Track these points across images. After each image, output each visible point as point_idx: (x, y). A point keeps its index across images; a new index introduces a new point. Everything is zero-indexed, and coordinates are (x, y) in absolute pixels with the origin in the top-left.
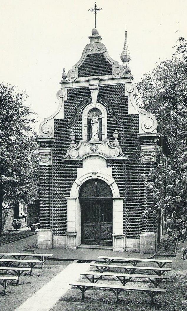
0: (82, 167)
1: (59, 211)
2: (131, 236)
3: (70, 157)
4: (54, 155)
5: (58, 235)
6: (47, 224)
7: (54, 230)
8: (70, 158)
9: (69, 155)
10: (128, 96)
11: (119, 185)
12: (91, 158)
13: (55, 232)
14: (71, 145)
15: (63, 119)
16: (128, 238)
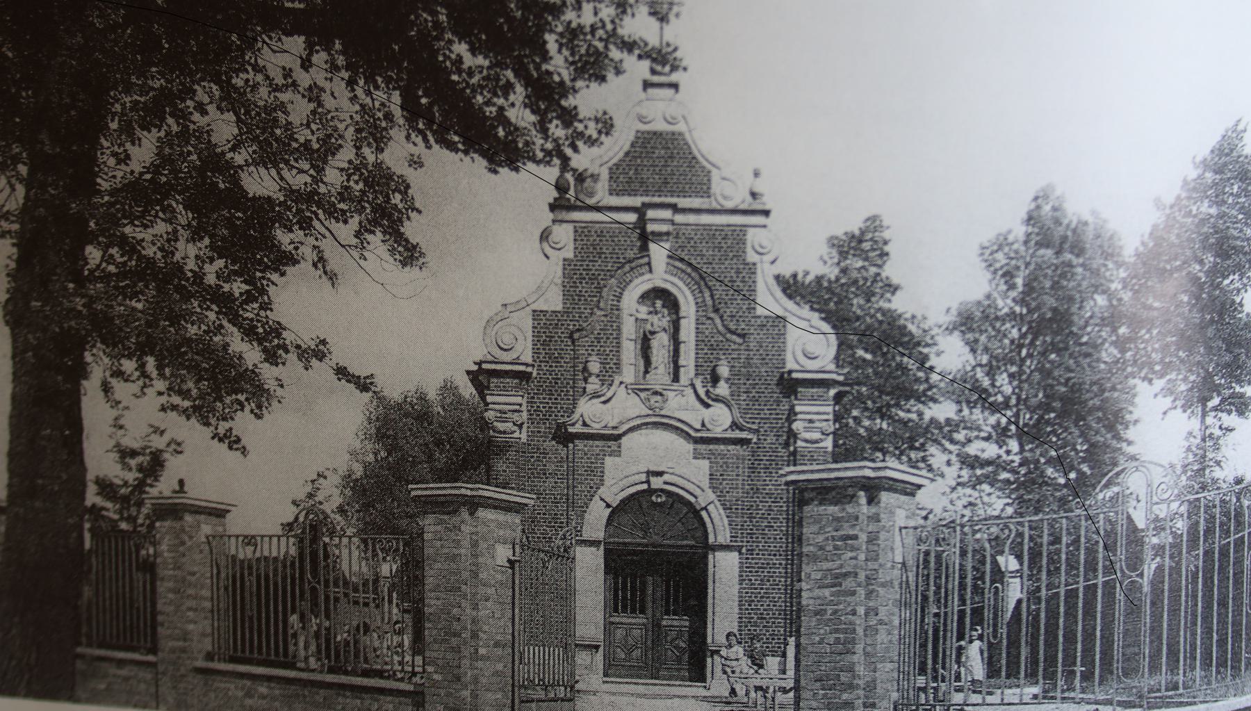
3: (584, 421)
8: (585, 424)
10: (754, 264)
12: (665, 429)
14: (590, 388)
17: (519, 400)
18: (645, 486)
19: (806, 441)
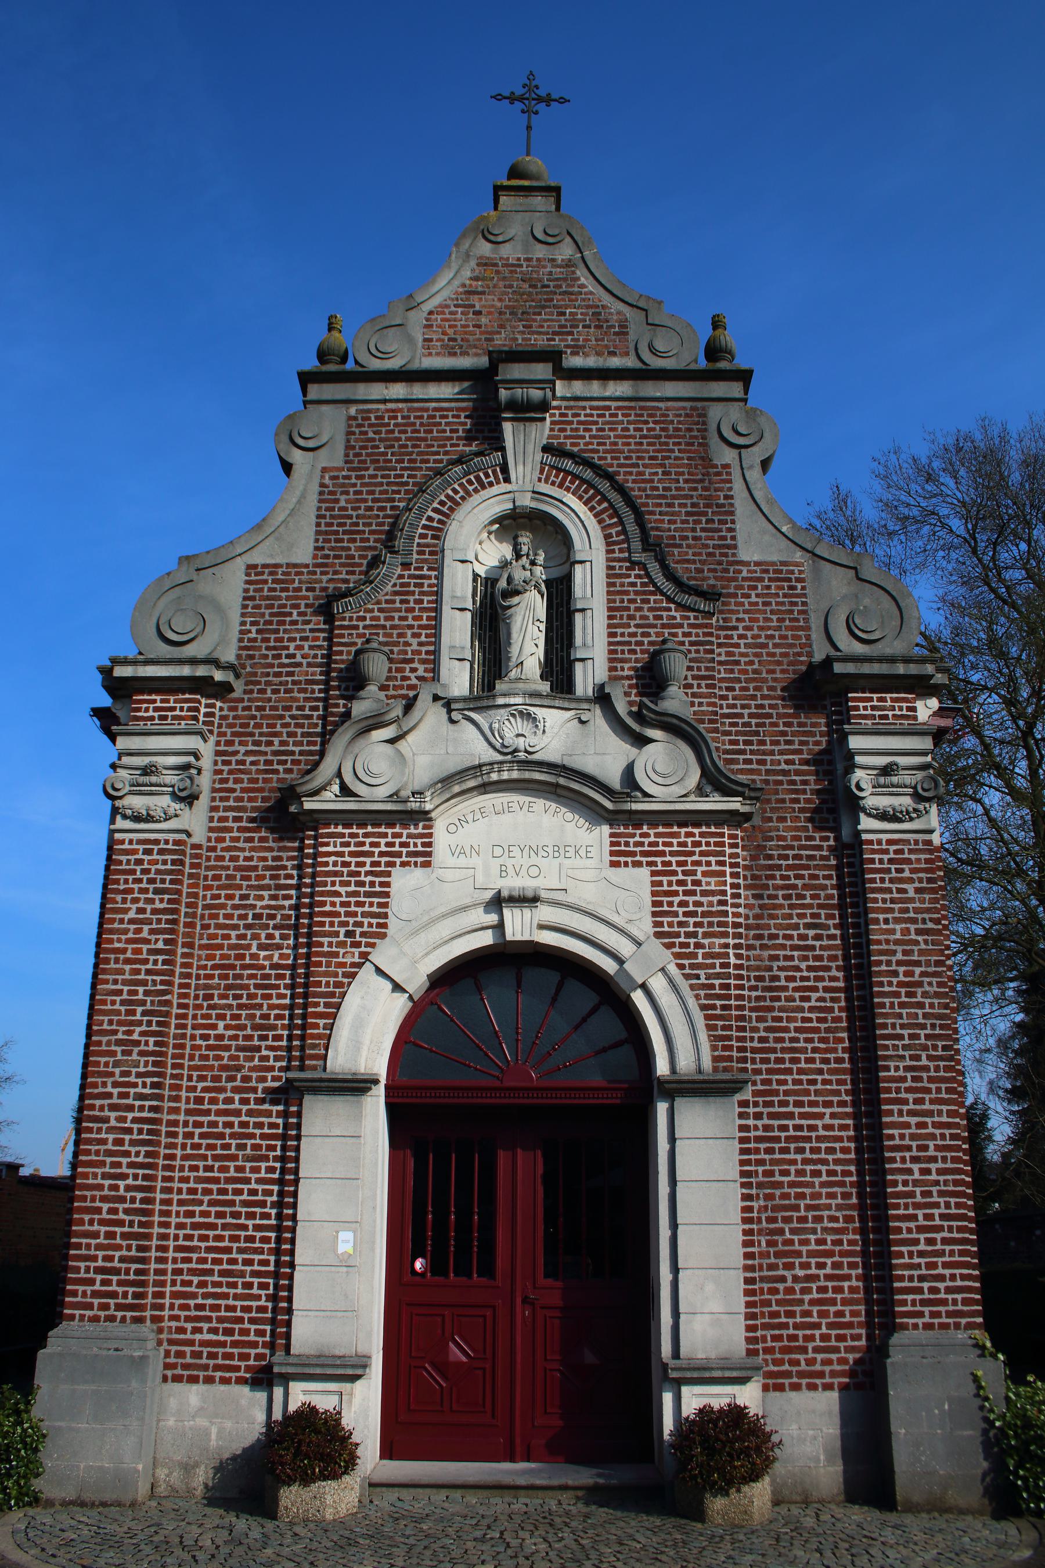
0: (427, 864)
1: (228, 1180)
2: (801, 1374)
4: (225, 781)
5: (209, 1380)
6: (120, 1283)
7: (171, 1342)
8: (346, 791)
9: (339, 774)
10: (726, 466)
11: (704, 986)
13: (180, 1354)
15: (307, 566)
16: (780, 1388)
17: (192, 742)
18: (487, 939)
19: (883, 816)
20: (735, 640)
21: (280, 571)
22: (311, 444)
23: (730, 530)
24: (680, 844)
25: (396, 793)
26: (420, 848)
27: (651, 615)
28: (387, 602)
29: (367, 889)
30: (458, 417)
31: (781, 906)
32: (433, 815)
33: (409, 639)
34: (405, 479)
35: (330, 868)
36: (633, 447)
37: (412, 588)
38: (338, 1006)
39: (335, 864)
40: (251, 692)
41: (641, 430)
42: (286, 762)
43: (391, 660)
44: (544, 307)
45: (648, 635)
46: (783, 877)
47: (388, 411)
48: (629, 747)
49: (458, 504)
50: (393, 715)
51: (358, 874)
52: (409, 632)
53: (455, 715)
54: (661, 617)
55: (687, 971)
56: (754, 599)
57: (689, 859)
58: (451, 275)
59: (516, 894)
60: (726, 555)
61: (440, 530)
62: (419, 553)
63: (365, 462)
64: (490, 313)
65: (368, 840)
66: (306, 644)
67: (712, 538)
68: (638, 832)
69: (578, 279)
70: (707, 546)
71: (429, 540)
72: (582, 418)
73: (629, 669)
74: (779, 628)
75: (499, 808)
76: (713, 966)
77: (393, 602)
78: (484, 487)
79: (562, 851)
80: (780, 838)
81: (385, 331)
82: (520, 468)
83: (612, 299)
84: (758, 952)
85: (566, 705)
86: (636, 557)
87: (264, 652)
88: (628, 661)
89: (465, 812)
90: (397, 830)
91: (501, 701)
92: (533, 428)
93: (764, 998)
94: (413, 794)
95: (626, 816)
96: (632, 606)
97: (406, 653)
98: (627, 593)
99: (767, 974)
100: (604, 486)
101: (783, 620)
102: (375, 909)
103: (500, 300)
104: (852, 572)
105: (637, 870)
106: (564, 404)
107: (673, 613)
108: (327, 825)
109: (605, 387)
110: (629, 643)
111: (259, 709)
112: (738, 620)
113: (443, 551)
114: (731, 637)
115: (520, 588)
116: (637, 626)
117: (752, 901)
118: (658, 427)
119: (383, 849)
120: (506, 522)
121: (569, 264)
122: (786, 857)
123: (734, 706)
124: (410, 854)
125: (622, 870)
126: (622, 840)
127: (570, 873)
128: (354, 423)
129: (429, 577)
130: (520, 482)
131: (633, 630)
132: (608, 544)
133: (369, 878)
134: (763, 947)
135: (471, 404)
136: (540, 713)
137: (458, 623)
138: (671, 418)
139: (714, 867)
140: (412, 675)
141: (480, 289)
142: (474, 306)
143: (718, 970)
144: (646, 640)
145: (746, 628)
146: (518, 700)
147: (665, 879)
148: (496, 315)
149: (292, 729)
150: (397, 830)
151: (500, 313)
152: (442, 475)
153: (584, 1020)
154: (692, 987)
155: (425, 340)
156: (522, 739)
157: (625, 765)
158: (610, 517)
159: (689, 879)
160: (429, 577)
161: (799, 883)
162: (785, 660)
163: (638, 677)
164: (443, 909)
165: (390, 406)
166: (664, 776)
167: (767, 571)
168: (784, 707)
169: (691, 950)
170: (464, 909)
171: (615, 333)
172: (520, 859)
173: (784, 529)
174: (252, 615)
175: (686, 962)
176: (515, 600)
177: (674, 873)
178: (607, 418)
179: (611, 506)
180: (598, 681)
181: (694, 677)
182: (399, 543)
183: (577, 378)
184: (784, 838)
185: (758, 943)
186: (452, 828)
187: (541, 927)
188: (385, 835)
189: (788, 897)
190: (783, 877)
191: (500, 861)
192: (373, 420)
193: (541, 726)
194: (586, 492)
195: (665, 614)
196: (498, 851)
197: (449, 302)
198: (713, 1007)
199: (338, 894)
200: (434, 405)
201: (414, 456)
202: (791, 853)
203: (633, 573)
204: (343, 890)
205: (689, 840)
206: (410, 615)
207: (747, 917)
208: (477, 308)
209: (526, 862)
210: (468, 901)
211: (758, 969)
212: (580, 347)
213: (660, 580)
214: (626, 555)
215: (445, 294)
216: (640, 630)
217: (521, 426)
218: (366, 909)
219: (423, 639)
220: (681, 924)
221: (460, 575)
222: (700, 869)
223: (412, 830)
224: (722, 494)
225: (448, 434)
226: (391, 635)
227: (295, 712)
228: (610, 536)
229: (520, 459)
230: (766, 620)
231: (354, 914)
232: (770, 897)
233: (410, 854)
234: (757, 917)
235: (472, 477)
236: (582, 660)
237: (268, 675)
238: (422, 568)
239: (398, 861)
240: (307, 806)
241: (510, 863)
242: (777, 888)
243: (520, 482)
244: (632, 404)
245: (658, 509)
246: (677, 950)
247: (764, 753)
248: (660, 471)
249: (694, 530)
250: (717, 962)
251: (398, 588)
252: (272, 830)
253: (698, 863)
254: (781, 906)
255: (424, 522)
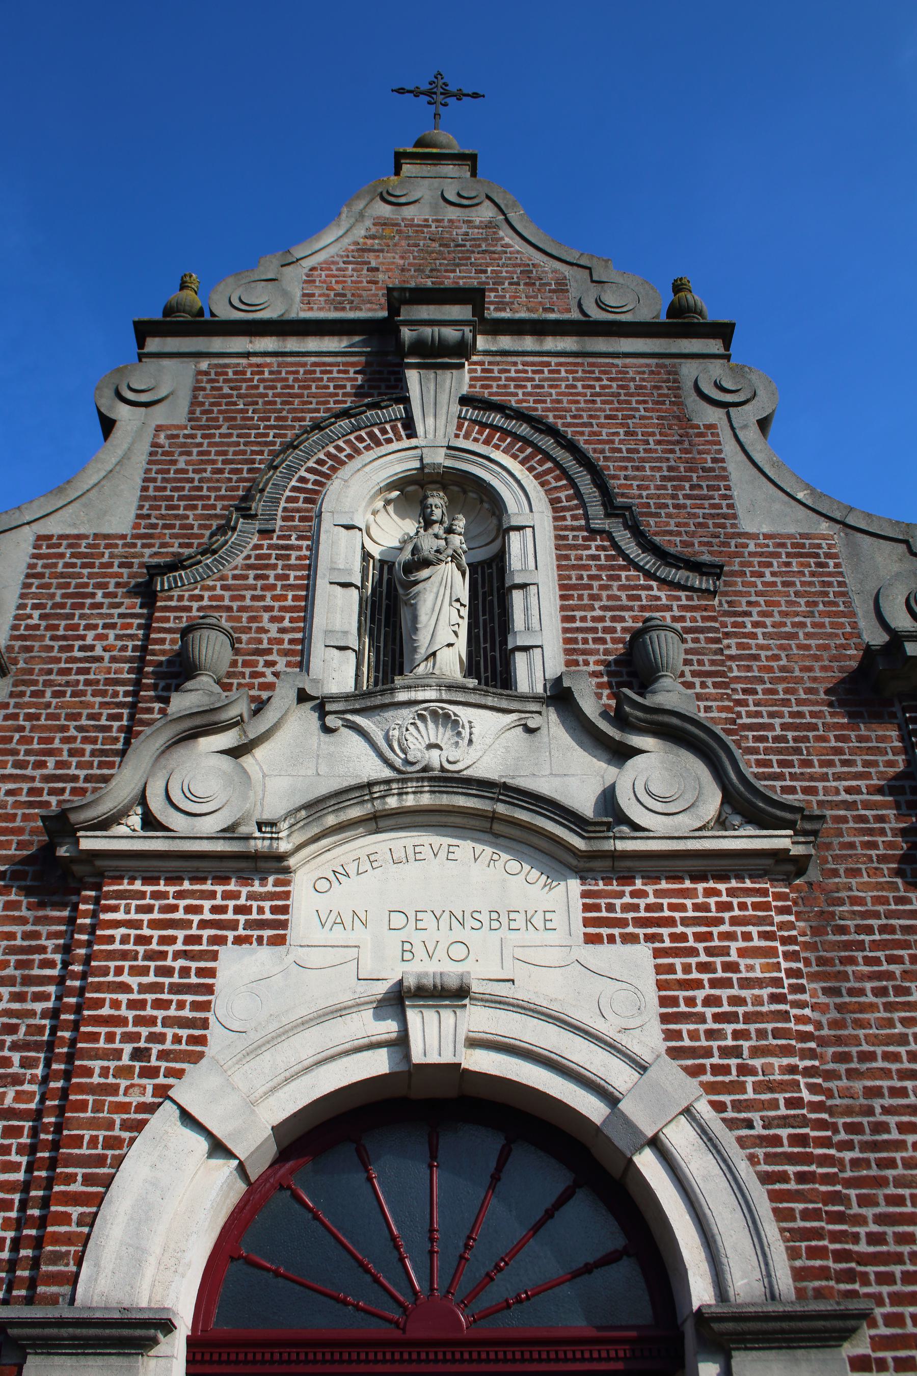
0: (279, 941)
8: (150, 822)
9: (142, 800)
11: (763, 1141)
15: (123, 537)
20: (749, 629)
21: (84, 543)
22: (143, 398)
23: (725, 497)
24: (696, 907)
25: (231, 828)
26: (268, 915)
27: (623, 595)
28: (235, 577)
29: (176, 979)
30: (346, 372)
31: (872, 1007)
32: (292, 862)
33: (265, 624)
34: (270, 438)
35: (117, 946)
36: (582, 405)
37: (273, 561)
38: (107, 1181)
39: (125, 940)
40: (22, 694)
41: (593, 387)
42: (62, 791)
43: (237, 651)
44: (458, 265)
45: (622, 619)
46: (868, 961)
47: (251, 365)
48: (604, 765)
49: (343, 463)
50: (232, 713)
51: (163, 955)
52: (266, 616)
53: (331, 721)
54: (639, 598)
55: (730, 1114)
56: (768, 578)
57: (715, 930)
58: (341, 233)
59: (428, 982)
60: (723, 526)
61: (317, 492)
62: (284, 519)
63: (217, 419)
64: (388, 270)
65: (182, 903)
66: (111, 634)
67: (701, 507)
68: (628, 889)
69: (502, 239)
70: (695, 516)
71: (300, 504)
72: (513, 374)
73: (597, 663)
74: (811, 614)
75: (399, 854)
76: (774, 1104)
77: (246, 577)
78: (378, 444)
79: (504, 919)
80: (855, 901)
81: (253, 285)
82: (430, 421)
83: (546, 258)
84: (844, 1083)
85: (504, 704)
86: (596, 524)
87: (48, 642)
88: (597, 652)
89: (343, 860)
90: (232, 887)
91: (402, 696)
92: (447, 376)
93: (866, 1163)
94: (260, 825)
95: (608, 863)
96: (596, 584)
97: (260, 641)
98: (586, 568)
99: (865, 1120)
100: (547, 443)
101: (815, 604)
102: (186, 1013)
103: (402, 258)
104: (902, 548)
105: (629, 948)
106: (488, 359)
107: (655, 592)
108: (118, 879)
109: (541, 342)
110: (594, 630)
111: (29, 717)
112: (749, 603)
113: (319, 516)
114: (743, 625)
115: (431, 557)
116: (604, 608)
117: (823, 999)
118: (614, 385)
119: (207, 916)
120: (411, 488)
121: (490, 225)
122: (869, 930)
123: (758, 714)
124: (249, 925)
125: (605, 949)
126: (603, 902)
127: (519, 953)
128: (205, 378)
129: (300, 548)
130: (430, 436)
131: (598, 613)
132: (555, 510)
133: (181, 963)
134: (852, 1074)
135: (363, 359)
136: (464, 714)
137: (339, 602)
138: (631, 375)
139: (757, 942)
140: (268, 671)
141: (376, 247)
142: (369, 263)
143: (783, 1111)
144: (619, 626)
145: (762, 614)
146: (431, 694)
147: (678, 962)
148: (397, 272)
149: (78, 745)
150: (232, 887)
151: (403, 270)
152: (322, 429)
153: (549, 1214)
154: (742, 1142)
155: (304, 295)
156: (435, 753)
157: (599, 790)
158: (557, 479)
159: (718, 961)
160: (300, 548)
161: (896, 969)
162: (825, 655)
163: (610, 674)
164: (303, 1011)
165: (254, 360)
166: (664, 800)
167: (783, 545)
168: (832, 715)
169: (733, 1076)
170: (339, 1011)
171: (550, 291)
172: (433, 932)
173: (800, 496)
174: (35, 596)
175: (727, 1098)
176: (425, 573)
177: (693, 952)
178: (546, 374)
179: (558, 465)
180: (552, 673)
181: (694, 674)
182: (258, 506)
183: (504, 333)
184: (860, 901)
185: (842, 1068)
186: (323, 885)
187: (473, 1043)
188: (212, 895)
189: (881, 992)
190: (868, 961)
191: (402, 935)
192: (231, 375)
193: (465, 733)
194: (521, 450)
195: (643, 594)
196: (398, 920)
197: (336, 259)
198: (783, 1177)
199: (126, 988)
200: (313, 359)
201: (284, 414)
202: (875, 923)
203: (593, 544)
204: (134, 981)
205: (712, 901)
206: (268, 594)
207: (818, 1025)
208: (373, 264)
209: (445, 936)
210: (345, 997)
211: (848, 1111)
212: (507, 303)
213: (633, 550)
214: (583, 522)
215: (332, 250)
216: (609, 614)
217: (431, 374)
218: (172, 1012)
219: (286, 624)
220: (711, 1034)
221: (343, 544)
222: (734, 946)
223: (257, 887)
224: (708, 457)
225: (332, 390)
226: (239, 619)
227: (84, 722)
228: (559, 500)
229: (430, 410)
230: (790, 603)
231: (152, 1021)
232: (851, 992)
233: (249, 925)
234: (834, 1024)
235: (363, 433)
236: (526, 649)
237: (50, 672)
238: (289, 537)
239: (230, 935)
240: (86, 844)
241: (417, 938)
242: (861, 977)
243: (430, 436)
244: (579, 360)
245: (622, 473)
246: (708, 1078)
247: (812, 778)
248: (621, 431)
249: (675, 497)
250: (781, 1097)
251: (252, 561)
252: (28, 891)
253: (730, 936)
254: (872, 1007)
255: (293, 483)
